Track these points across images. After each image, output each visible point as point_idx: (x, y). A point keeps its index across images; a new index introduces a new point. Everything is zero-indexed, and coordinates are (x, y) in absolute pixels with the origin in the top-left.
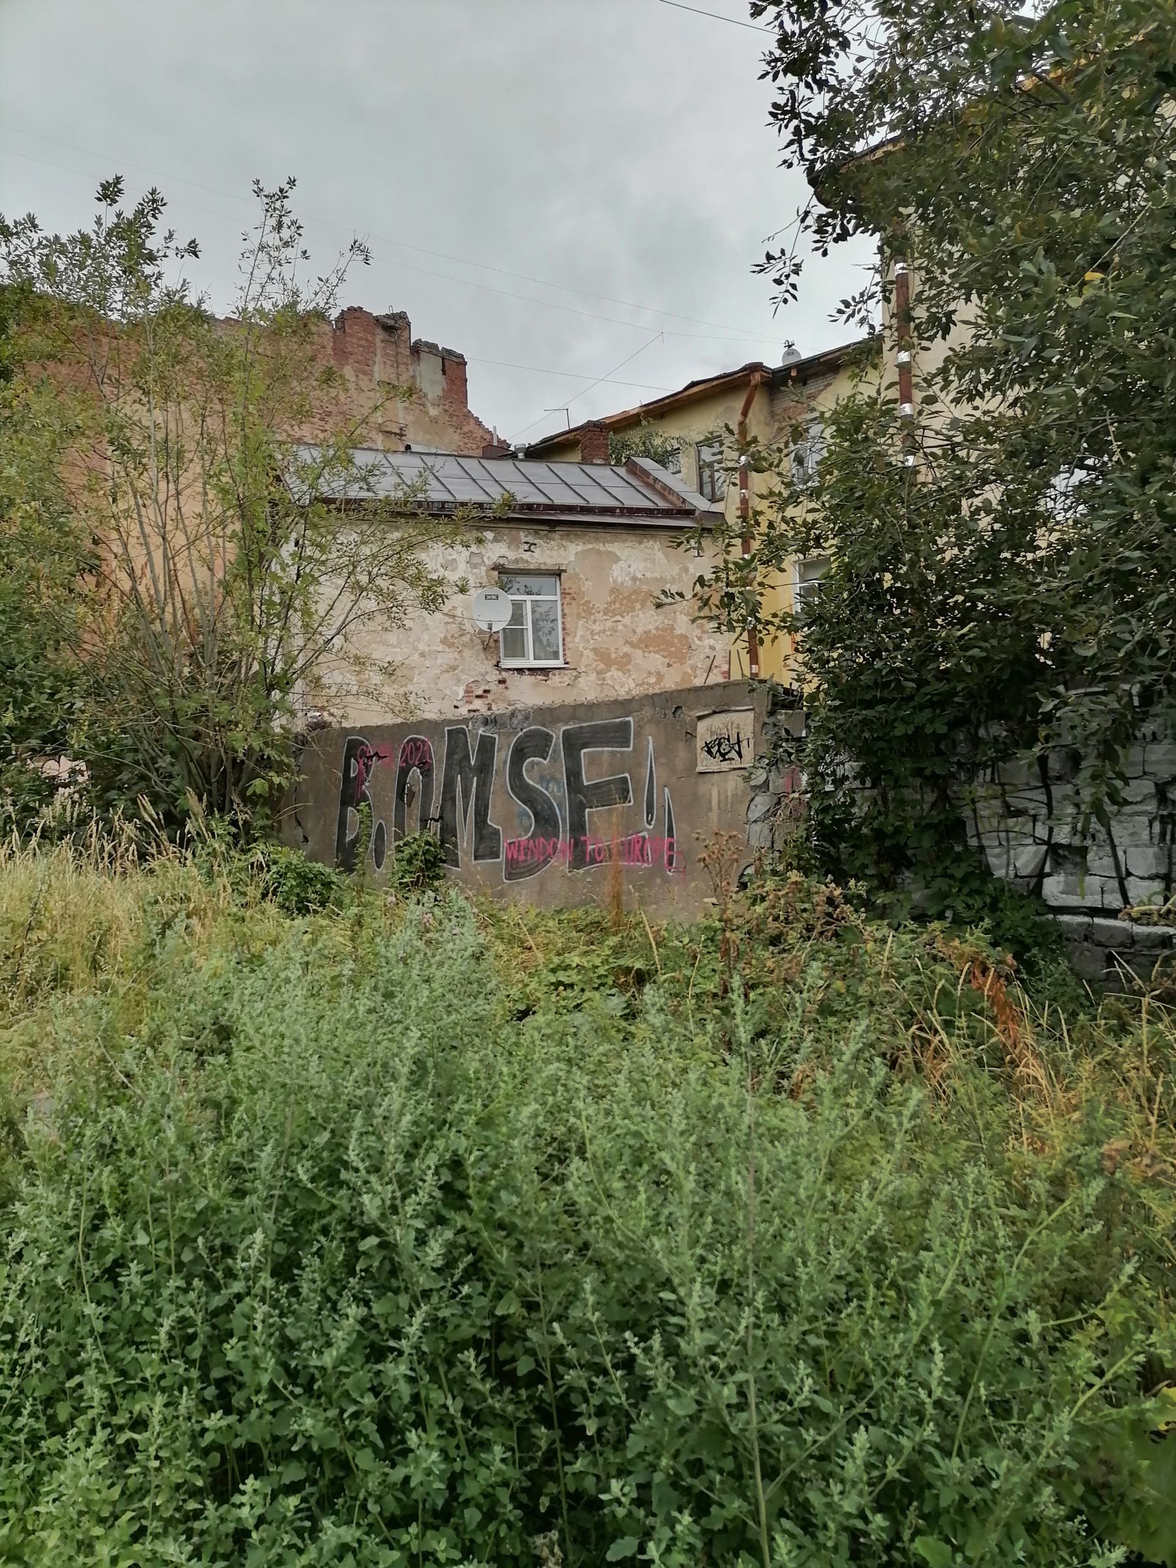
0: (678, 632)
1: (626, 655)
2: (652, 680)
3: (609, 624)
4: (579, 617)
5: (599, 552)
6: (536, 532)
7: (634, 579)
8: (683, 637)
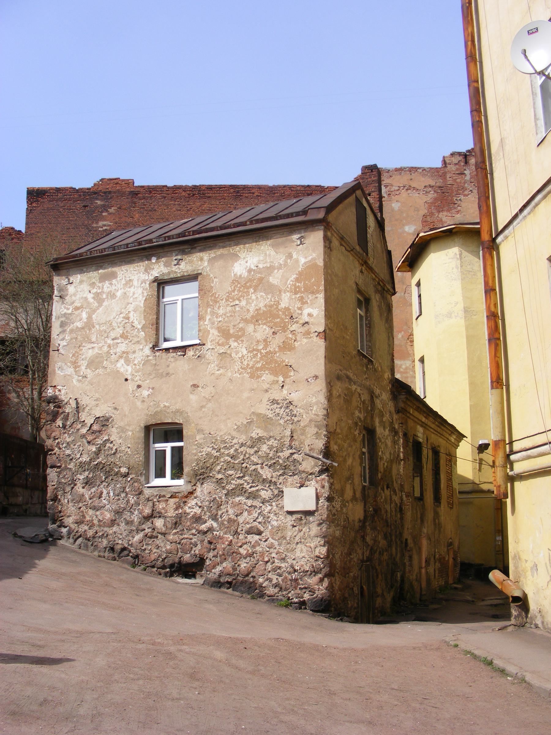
0: (283, 305)
1: (242, 329)
3: (229, 308)
4: (208, 305)
7: (250, 271)
8: (287, 309)
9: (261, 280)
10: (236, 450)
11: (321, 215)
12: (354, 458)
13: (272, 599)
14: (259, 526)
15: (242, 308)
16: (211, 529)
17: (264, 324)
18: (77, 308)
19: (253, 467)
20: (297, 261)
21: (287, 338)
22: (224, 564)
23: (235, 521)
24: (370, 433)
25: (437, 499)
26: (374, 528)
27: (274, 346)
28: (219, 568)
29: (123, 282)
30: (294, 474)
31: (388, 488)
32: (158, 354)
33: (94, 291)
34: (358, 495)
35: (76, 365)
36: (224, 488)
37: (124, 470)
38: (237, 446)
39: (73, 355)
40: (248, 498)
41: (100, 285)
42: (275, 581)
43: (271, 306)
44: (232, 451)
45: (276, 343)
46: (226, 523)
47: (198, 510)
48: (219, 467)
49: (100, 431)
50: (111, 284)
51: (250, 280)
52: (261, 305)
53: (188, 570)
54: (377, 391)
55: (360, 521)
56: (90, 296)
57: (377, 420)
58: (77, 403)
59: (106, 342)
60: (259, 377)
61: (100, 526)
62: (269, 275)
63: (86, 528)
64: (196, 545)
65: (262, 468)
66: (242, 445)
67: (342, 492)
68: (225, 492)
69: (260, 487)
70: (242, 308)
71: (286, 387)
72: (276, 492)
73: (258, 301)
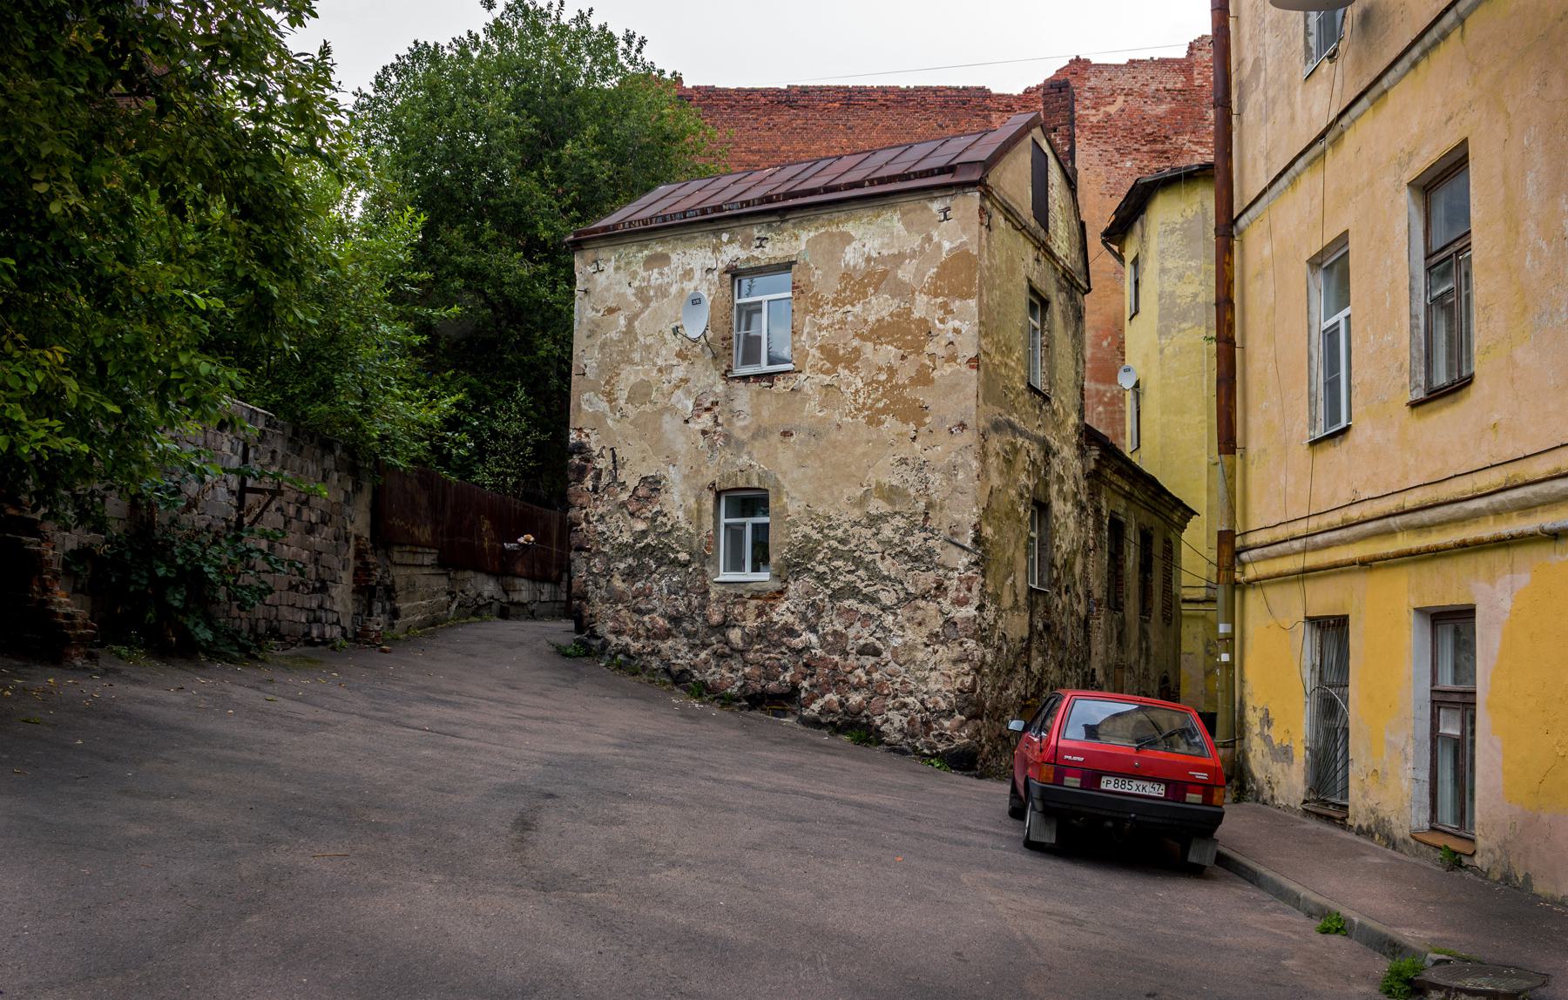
0: (916, 315)
1: (856, 350)
2: (883, 377)
3: (838, 316)
4: (806, 312)
5: (832, 235)
6: (769, 225)
7: (868, 259)
8: (923, 321)
9: (885, 274)
10: (846, 531)
11: (975, 177)
12: (1016, 546)
13: (894, 749)
14: (879, 644)
15: (856, 317)
16: (807, 648)
17: (888, 343)
18: (611, 311)
19: (870, 557)
20: (939, 246)
21: (923, 365)
22: (828, 697)
23: (842, 635)
24: (1041, 507)
25: (1145, 610)
26: (1043, 653)
27: (902, 379)
28: (820, 702)
29: (680, 272)
30: (928, 569)
31: (1067, 592)
32: (735, 384)
33: (636, 284)
34: (1022, 599)
35: (611, 398)
36: (827, 586)
37: (683, 556)
38: (847, 526)
39: (607, 383)
40: (862, 602)
41: (645, 274)
42: (897, 725)
43: (899, 315)
44: (839, 533)
45: (906, 373)
46: (830, 639)
47: (790, 619)
48: (820, 556)
49: (647, 498)
50: (661, 274)
51: (869, 274)
52: (884, 313)
53: (772, 701)
54: (1055, 444)
55: (1022, 640)
56: (630, 292)
57: (1054, 489)
58: (614, 456)
59: (655, 364)
60: (881, 423)
61: (648, 638)
62: (898, 267)
63: (628, 640)
64: (786, 669)
65: (883, 558)
66: (856, 523)
67: (996, 598)
68: (829, 592)
69: (878, 587)
70: (856, 317)
71: (919, 440)
72: (902, 595)
73: (880, 307)
